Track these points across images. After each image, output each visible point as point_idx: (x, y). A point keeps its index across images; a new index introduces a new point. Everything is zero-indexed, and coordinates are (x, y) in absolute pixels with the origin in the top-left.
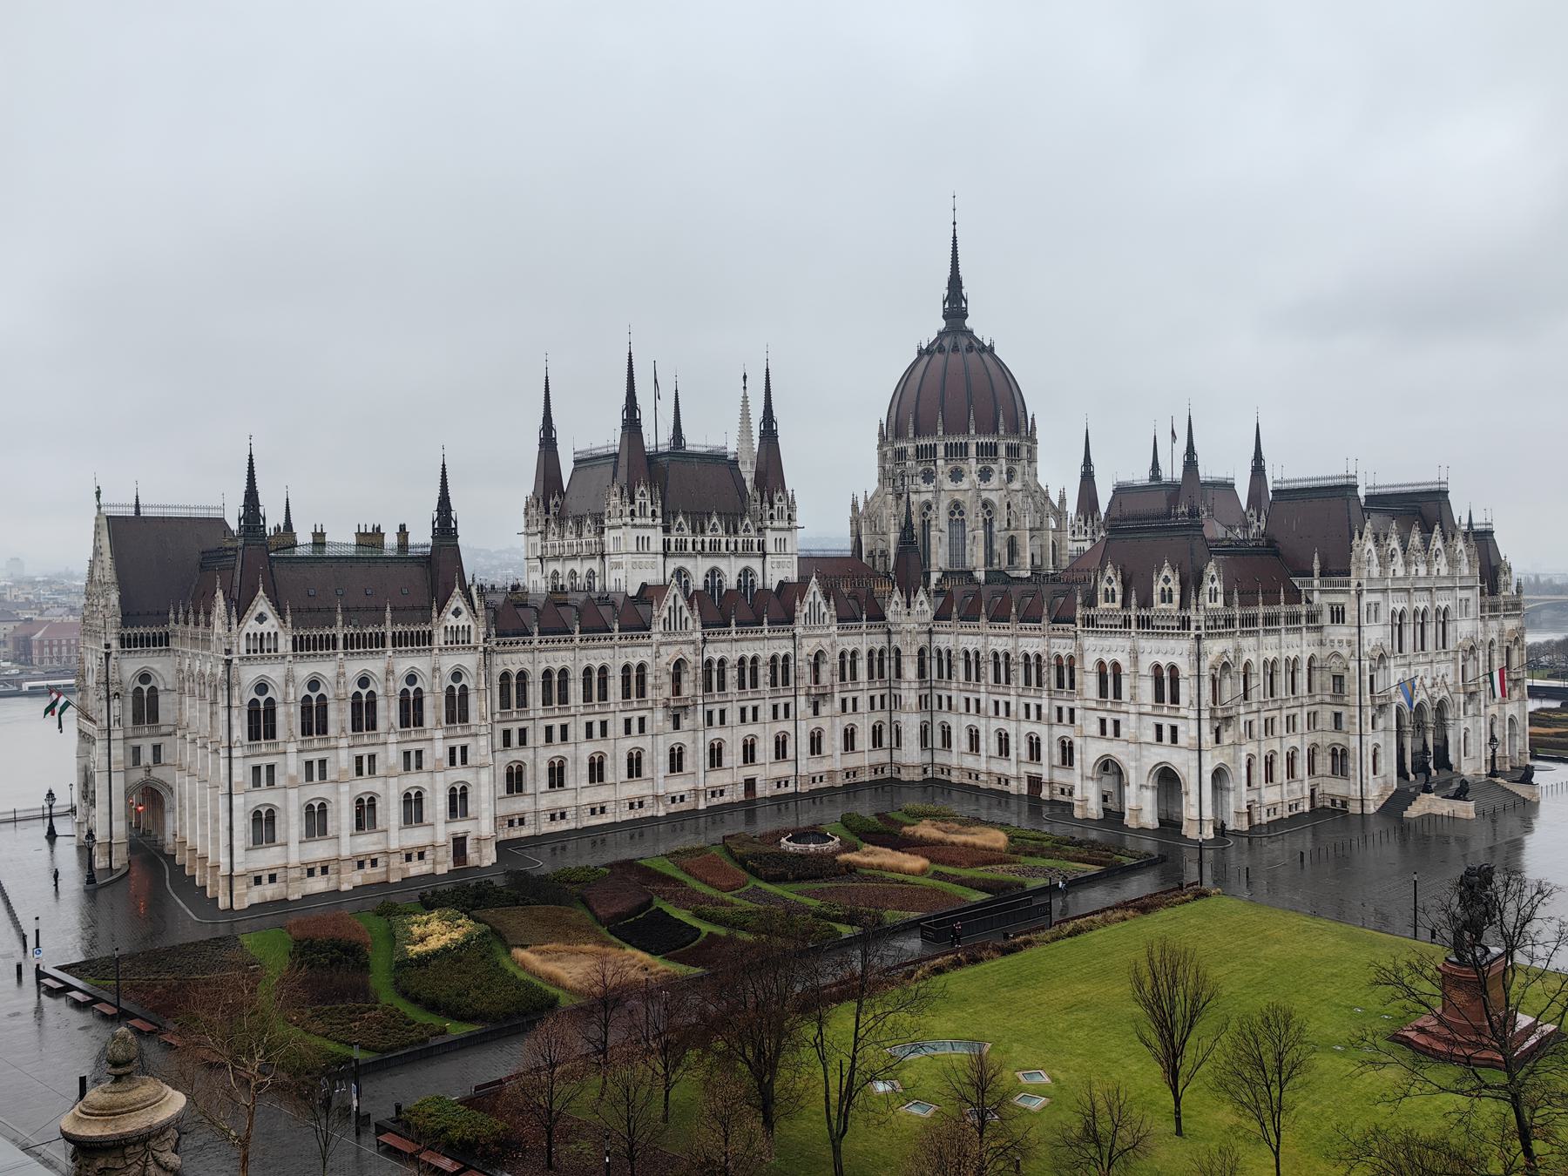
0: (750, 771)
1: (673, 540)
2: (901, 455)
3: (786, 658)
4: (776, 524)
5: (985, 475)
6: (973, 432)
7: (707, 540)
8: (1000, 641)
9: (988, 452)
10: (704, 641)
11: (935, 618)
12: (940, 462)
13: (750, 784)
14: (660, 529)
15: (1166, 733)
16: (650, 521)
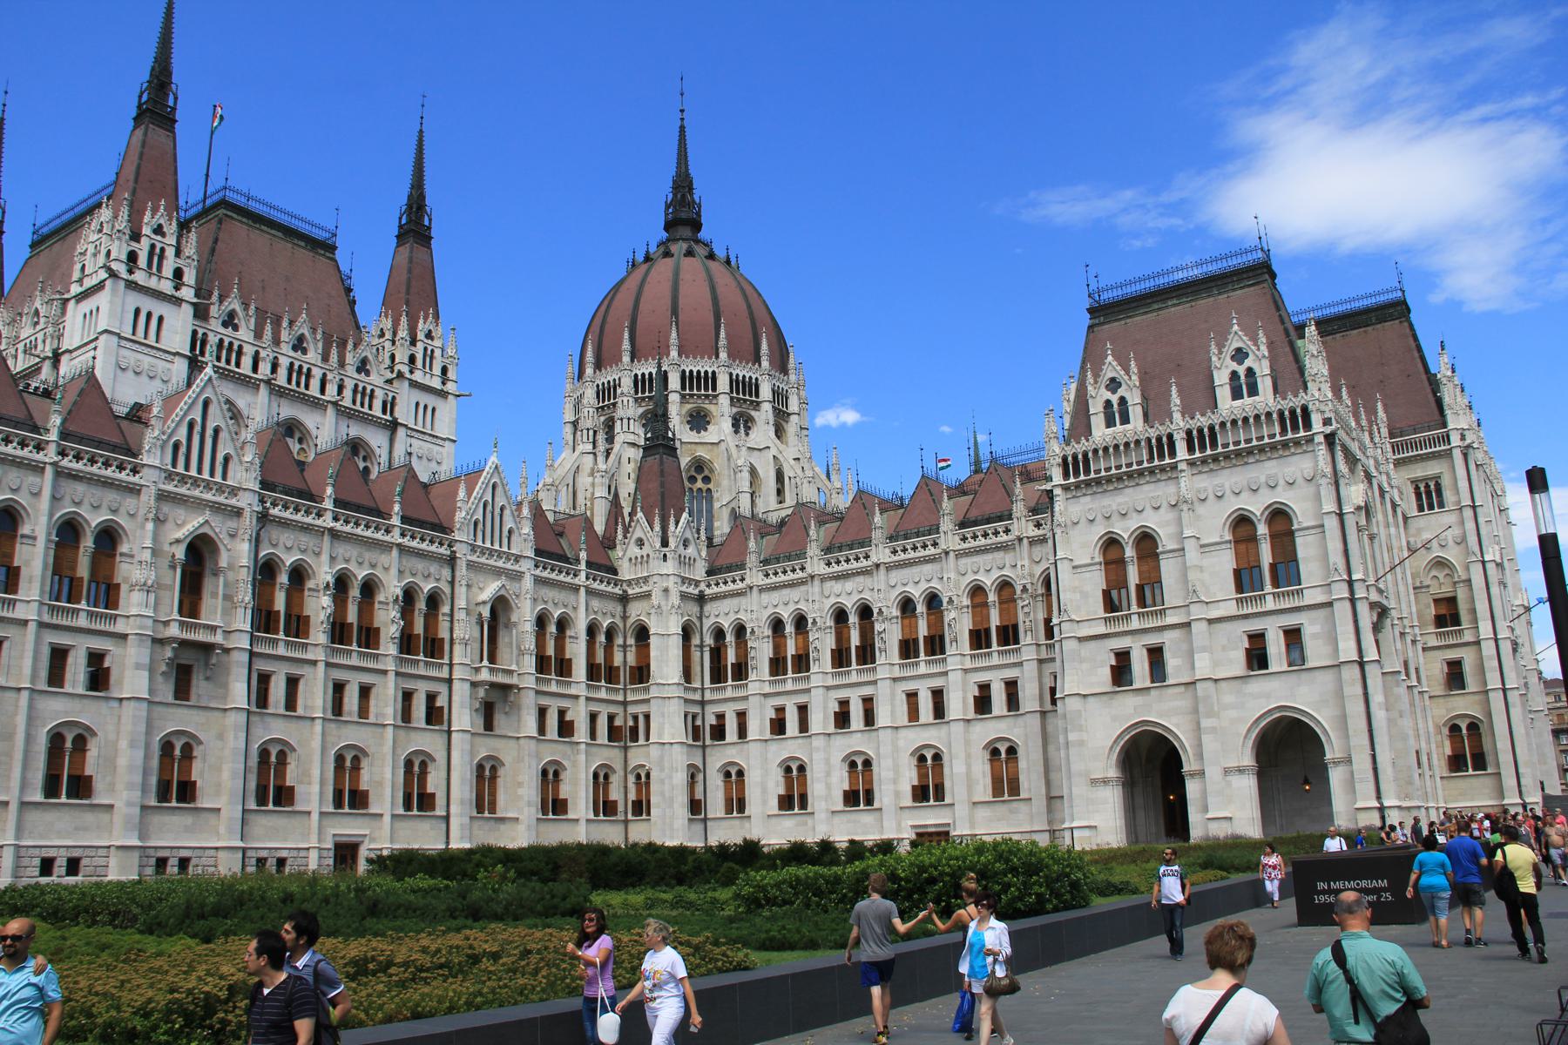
0: (349, 827)
1: (213, 339)
2: (607, 393)
3: (433, 600)
4: (418, 376)
5: (742, 422)
6: (723, 355)
7: (284, 362)
8: (849, 585)
9: (744, 390)
10: (264, 518)
11: (710, 573)
12: (674, 398)
13: (345, 852)
14: (187, 310)
15: (1276, 647)
16: (167, 287)
